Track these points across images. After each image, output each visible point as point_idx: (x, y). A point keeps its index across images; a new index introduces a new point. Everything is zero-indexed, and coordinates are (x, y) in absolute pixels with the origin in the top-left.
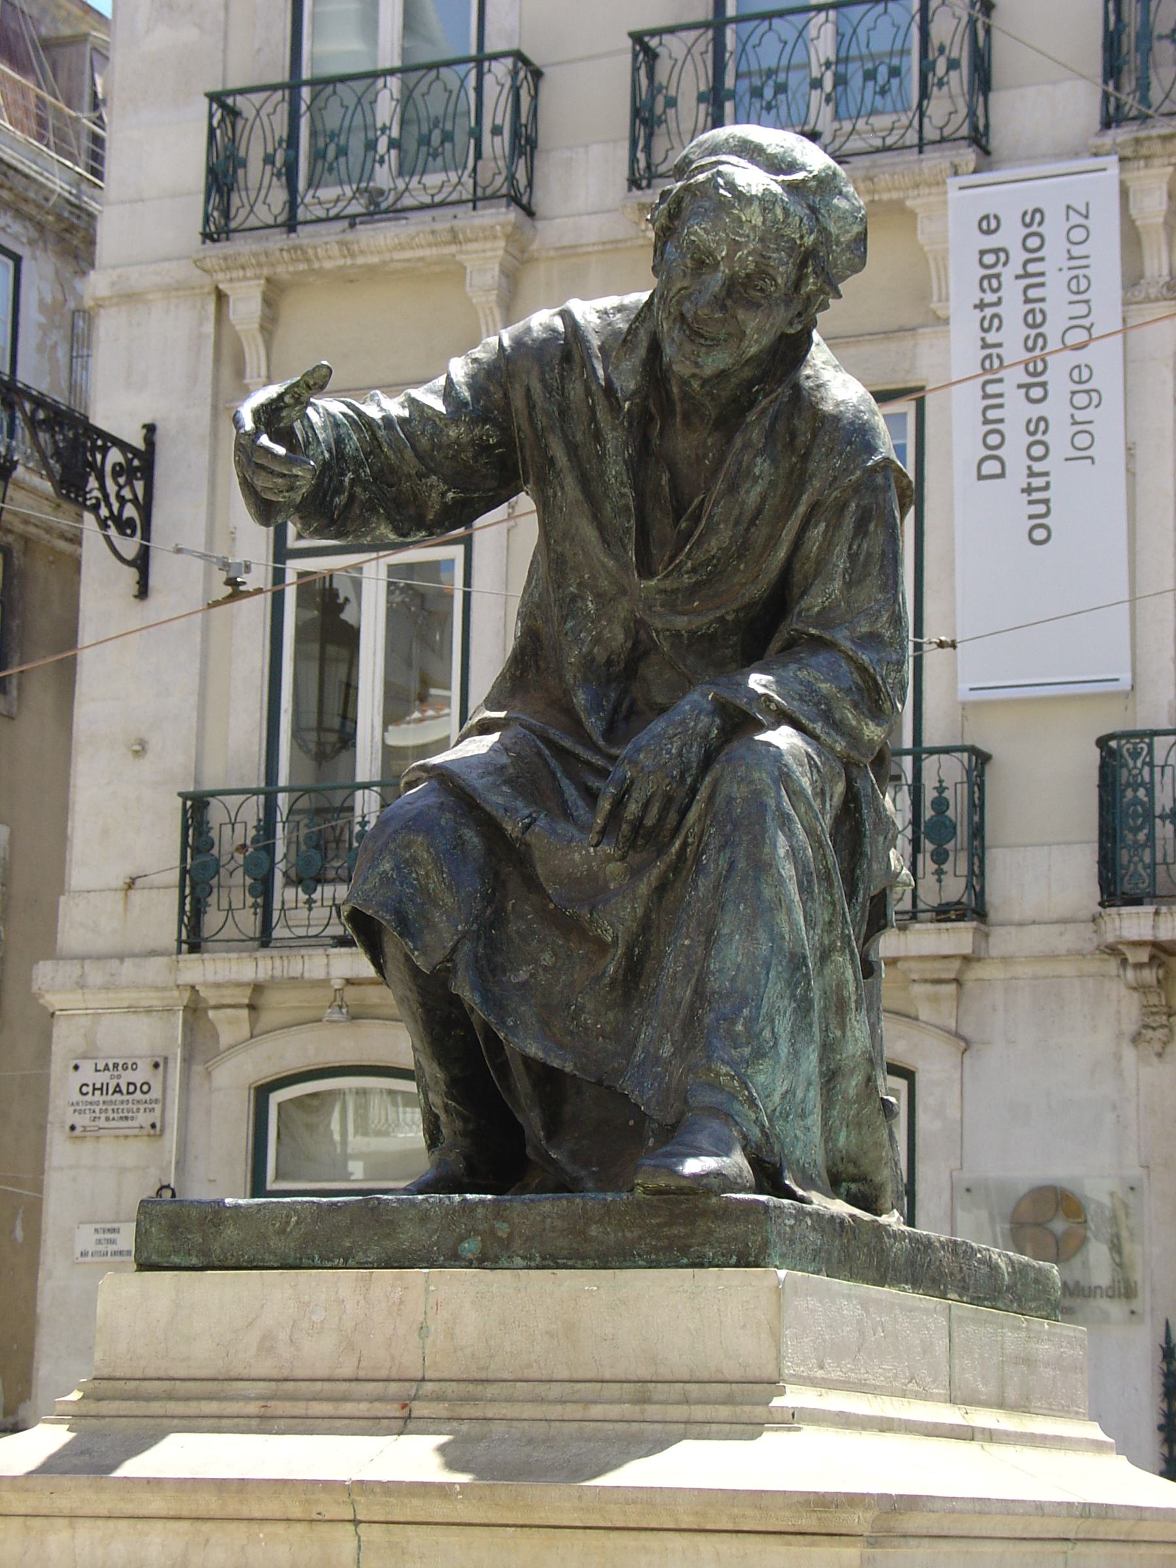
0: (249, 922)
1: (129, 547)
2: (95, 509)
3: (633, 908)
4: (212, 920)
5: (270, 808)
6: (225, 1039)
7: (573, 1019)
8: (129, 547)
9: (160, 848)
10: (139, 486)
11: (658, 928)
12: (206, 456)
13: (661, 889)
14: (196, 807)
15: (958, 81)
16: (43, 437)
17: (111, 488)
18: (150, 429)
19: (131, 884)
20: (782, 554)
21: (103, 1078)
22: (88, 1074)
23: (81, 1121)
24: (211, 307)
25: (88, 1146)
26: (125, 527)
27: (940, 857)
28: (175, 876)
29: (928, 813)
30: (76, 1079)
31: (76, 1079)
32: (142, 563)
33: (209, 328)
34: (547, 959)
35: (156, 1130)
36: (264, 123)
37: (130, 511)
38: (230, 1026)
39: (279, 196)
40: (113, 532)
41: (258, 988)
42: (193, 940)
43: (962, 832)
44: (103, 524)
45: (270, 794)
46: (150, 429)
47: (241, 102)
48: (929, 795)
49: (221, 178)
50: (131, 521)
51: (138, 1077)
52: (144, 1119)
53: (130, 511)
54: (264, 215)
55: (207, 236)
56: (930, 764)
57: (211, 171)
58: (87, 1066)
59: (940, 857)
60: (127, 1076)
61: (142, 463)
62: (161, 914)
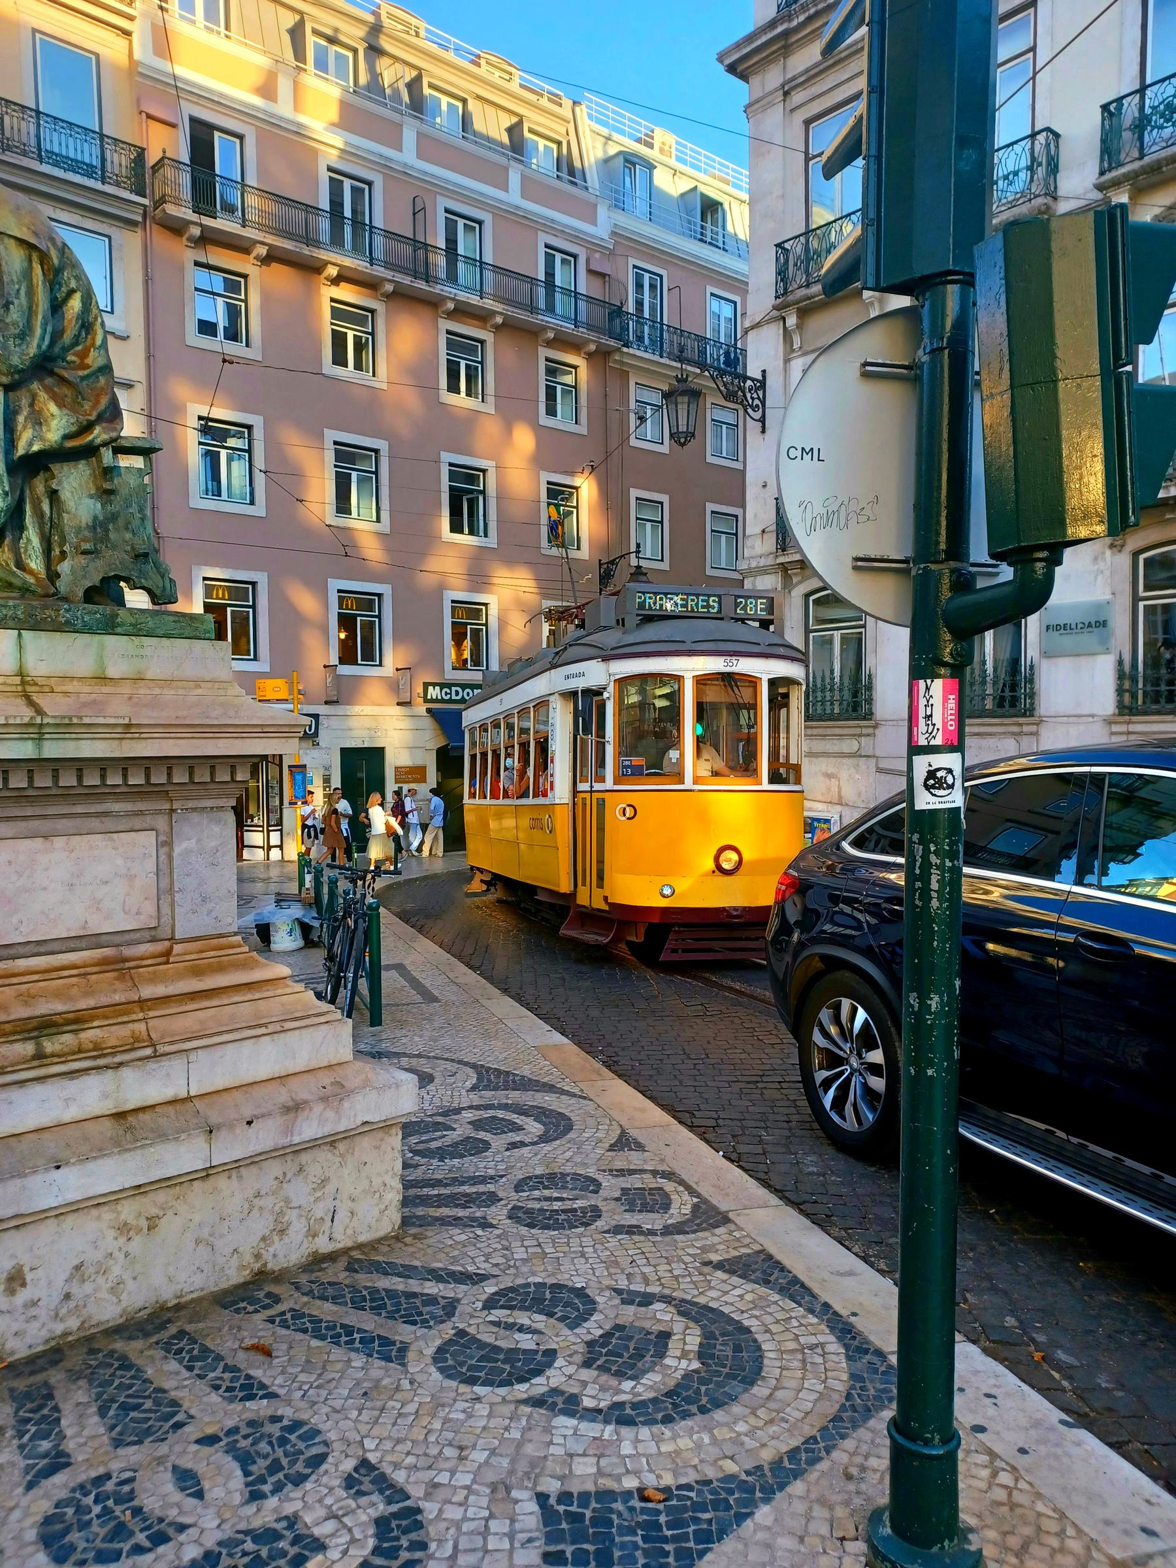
2: (741, 403)
6: (795, 580)
10: (761, 393)
12: (781, 379)
18: (764, 372)
32: (762, 420)
37: (757, 402)
46: (764, 372)
47: (787, 246)
53: (757, 402)
57: (779, 273)
61: (762, 384)
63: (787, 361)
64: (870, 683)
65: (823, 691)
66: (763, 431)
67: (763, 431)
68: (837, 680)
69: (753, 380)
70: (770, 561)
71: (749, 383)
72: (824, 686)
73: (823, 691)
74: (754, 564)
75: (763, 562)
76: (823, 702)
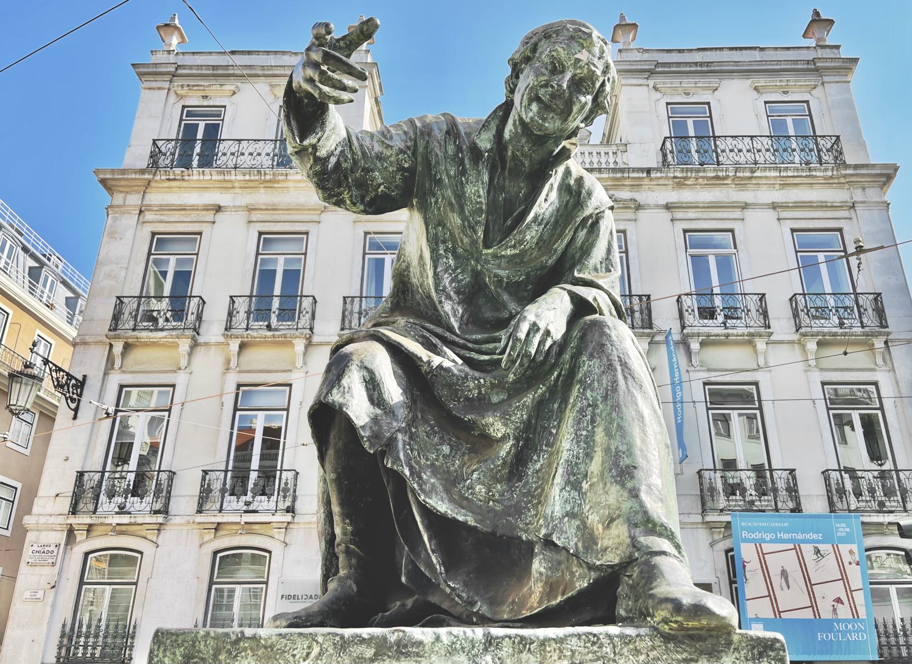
0: (91, 507)
1: (73, 406)
2: (65, 395)
3: (522, 415)
4: (81, 505)
5: (102, 476)
6: (78, 540)
7: (468, 489)
8: (73, 406)
9: (69, 487)
11: (535, 429)
12: (100, 384)
13: (540, 405)
14: (81, 474)
15: (308, 316)
16: (54, 374)
17: (71, 390)
18: (85, 376)
19: (57, 495)
20: (565, 242)
21: (38, 549)
22: (35, 548)
23: (30, 561)
24: (108, 347)
25: (33, 568)
26: (73, 400)
27: (285, 497)
28: (71, 494)
29: (282, 485)
30: (32, 549)
31: (32, 549)
32: (76, 410)
33: (106, 353)
34: (446, 449)
35: (53, 564)
36: (130, 306)
38: (80, 536)
39: (132, 323)
40: (69, 401)
41: (90, 525)
42: (74, 511)
43: (292, 491)
44: (67, 399)
45: (103, 472)
46: (85, 376)
48: (283, 481)
49: (116, 317)
50: (75, 399)
51: (50, 549)
52: (50, 561)
53: (75, 396)
54: (127, 326)
55: (110, 330)
56: (284, 473)
58: (35, 546)
59: (285, 497)
60: (48, 548)
62: (65, 504)
63: (106, 374)
64: (134, 632)
65: (87, 637)
66: (75, 418)
67: (75, 418)
68: (103, 628)
69: (76, 380)
70: (61, 520)
71: (73, 381)
72: (88, 632)
73: (87, 637)
74: (42, 520)
75: (52, 520)
76: (85, 647)
